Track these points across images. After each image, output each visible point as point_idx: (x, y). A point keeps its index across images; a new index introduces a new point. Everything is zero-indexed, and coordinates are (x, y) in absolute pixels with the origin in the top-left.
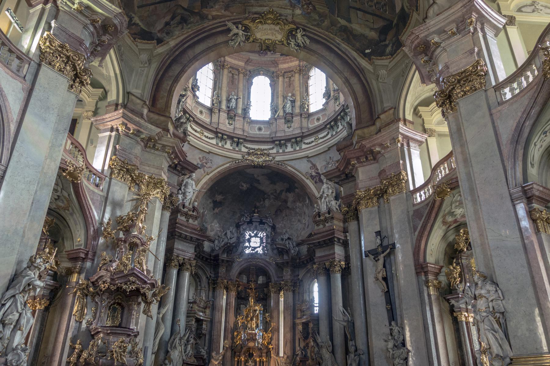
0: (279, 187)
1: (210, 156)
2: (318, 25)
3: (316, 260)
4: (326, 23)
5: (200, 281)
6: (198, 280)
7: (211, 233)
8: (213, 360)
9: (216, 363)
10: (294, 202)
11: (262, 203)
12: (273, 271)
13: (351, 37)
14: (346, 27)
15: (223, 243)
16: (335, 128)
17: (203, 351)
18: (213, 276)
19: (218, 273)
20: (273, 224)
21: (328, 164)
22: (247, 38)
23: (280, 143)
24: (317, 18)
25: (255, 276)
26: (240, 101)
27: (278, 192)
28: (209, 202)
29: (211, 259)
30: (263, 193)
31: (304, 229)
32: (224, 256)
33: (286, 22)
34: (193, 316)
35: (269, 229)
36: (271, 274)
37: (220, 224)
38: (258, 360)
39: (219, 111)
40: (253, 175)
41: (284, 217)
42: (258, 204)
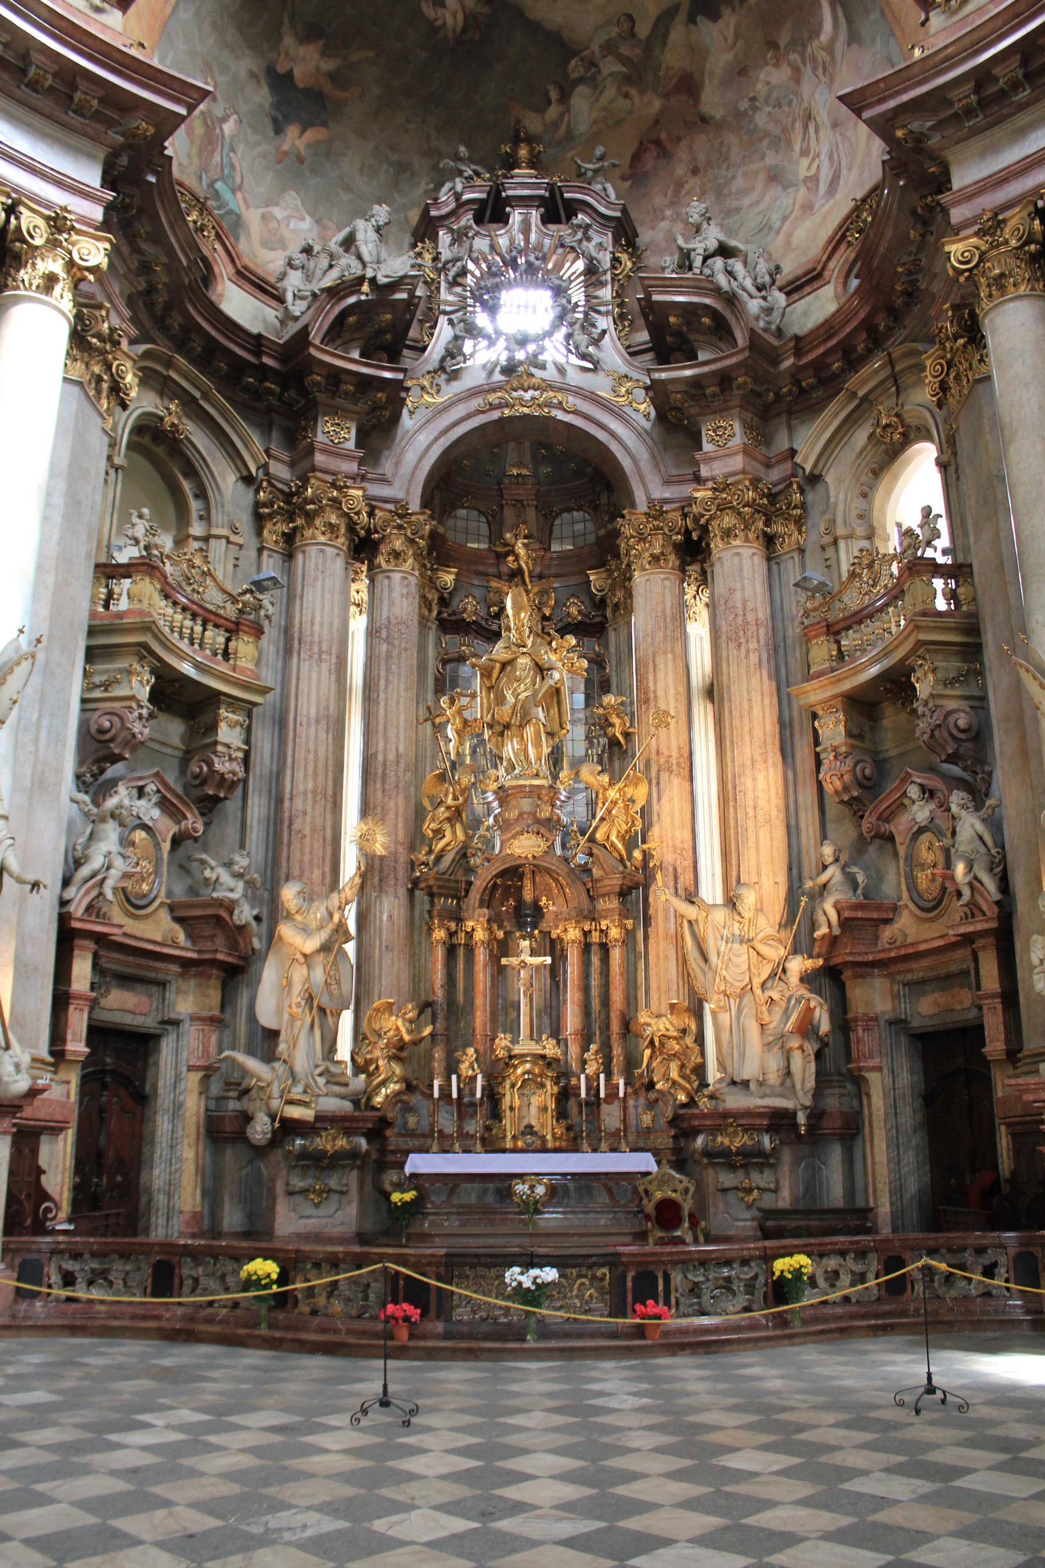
3: (957, 215)
5: (202, 494)
6: (186, 485)
8: (285, 930)
9: (310, 945)
10: (741, 71)
11: (553, 112)
12: (643, 455)
15: (335, 273)
17: (225, 878)
18: (280, 470)
19: (311, 450)
20: (624, 210)
25: (531, 514)
27: (643, 30)
28: (243, 74)
29: (263, 371)
31: (808, 208)
32: (351, 361)
34: (144, 652)
35: (601, 245)
36: (626, 462)
37: (318, 222)
38: (573, 934)
41: (680, 185)
42: (532, 123)
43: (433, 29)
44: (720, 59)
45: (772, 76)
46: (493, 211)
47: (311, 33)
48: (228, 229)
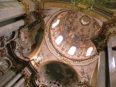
0: (69, 75)
1: (52, 55)
2: (98, 5)
4: (101, 3)
7: (40, 80)
11: (61, 79)
13: (109, 5)
14: (108, 3)
16: (93, 58)
21: (88, 69)
22: (76, 5)
23: (75, 60)
24: (98, 2)
26: (66, 48)
30: (63, 76)
33: (88, 4)
39: (60, 47)
40: (62, 68)
42: (60, 80)
43: (56, 72)
44: (71, 81)
45: (73, 83)
46: (55, 83)
47: (49, 70)
48: (39, 78)
